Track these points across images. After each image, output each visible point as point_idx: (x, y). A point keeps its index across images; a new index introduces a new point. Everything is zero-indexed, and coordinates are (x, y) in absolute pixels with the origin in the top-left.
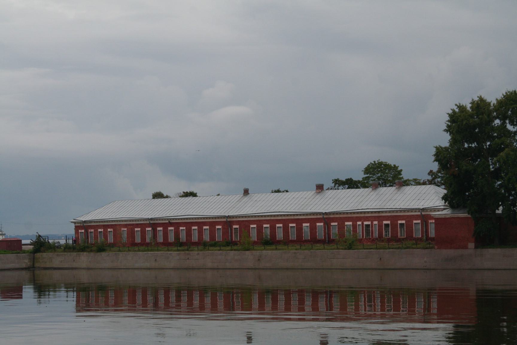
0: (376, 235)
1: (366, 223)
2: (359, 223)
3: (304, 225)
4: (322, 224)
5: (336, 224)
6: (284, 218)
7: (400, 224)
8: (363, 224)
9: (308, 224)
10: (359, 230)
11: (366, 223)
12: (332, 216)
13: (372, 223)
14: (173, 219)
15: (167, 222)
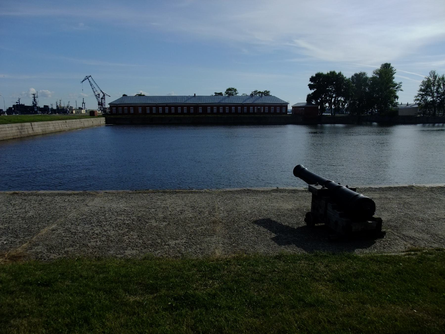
0: (262, 111)
1: (258, 107)
2: (256, 107)
3: (232, 107)
4: (240, 107)
5: (246, 107)
6: (223, 105)
7: (278, 108)
8: (257, 108)
9: (234, 107)
10: (256, 109)
11: (258, 107)
12: (245, 105)
13: (261, 108)
14: (169, 104)
15: (166, 105)
